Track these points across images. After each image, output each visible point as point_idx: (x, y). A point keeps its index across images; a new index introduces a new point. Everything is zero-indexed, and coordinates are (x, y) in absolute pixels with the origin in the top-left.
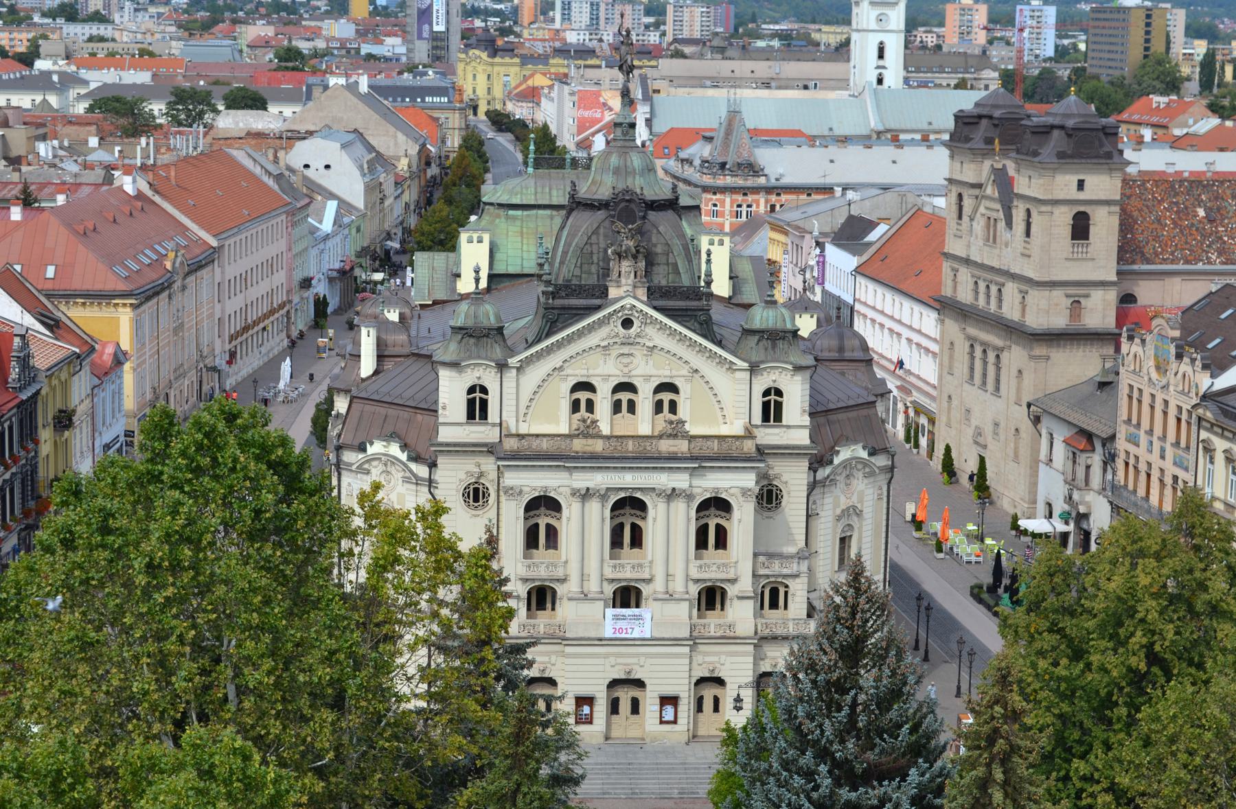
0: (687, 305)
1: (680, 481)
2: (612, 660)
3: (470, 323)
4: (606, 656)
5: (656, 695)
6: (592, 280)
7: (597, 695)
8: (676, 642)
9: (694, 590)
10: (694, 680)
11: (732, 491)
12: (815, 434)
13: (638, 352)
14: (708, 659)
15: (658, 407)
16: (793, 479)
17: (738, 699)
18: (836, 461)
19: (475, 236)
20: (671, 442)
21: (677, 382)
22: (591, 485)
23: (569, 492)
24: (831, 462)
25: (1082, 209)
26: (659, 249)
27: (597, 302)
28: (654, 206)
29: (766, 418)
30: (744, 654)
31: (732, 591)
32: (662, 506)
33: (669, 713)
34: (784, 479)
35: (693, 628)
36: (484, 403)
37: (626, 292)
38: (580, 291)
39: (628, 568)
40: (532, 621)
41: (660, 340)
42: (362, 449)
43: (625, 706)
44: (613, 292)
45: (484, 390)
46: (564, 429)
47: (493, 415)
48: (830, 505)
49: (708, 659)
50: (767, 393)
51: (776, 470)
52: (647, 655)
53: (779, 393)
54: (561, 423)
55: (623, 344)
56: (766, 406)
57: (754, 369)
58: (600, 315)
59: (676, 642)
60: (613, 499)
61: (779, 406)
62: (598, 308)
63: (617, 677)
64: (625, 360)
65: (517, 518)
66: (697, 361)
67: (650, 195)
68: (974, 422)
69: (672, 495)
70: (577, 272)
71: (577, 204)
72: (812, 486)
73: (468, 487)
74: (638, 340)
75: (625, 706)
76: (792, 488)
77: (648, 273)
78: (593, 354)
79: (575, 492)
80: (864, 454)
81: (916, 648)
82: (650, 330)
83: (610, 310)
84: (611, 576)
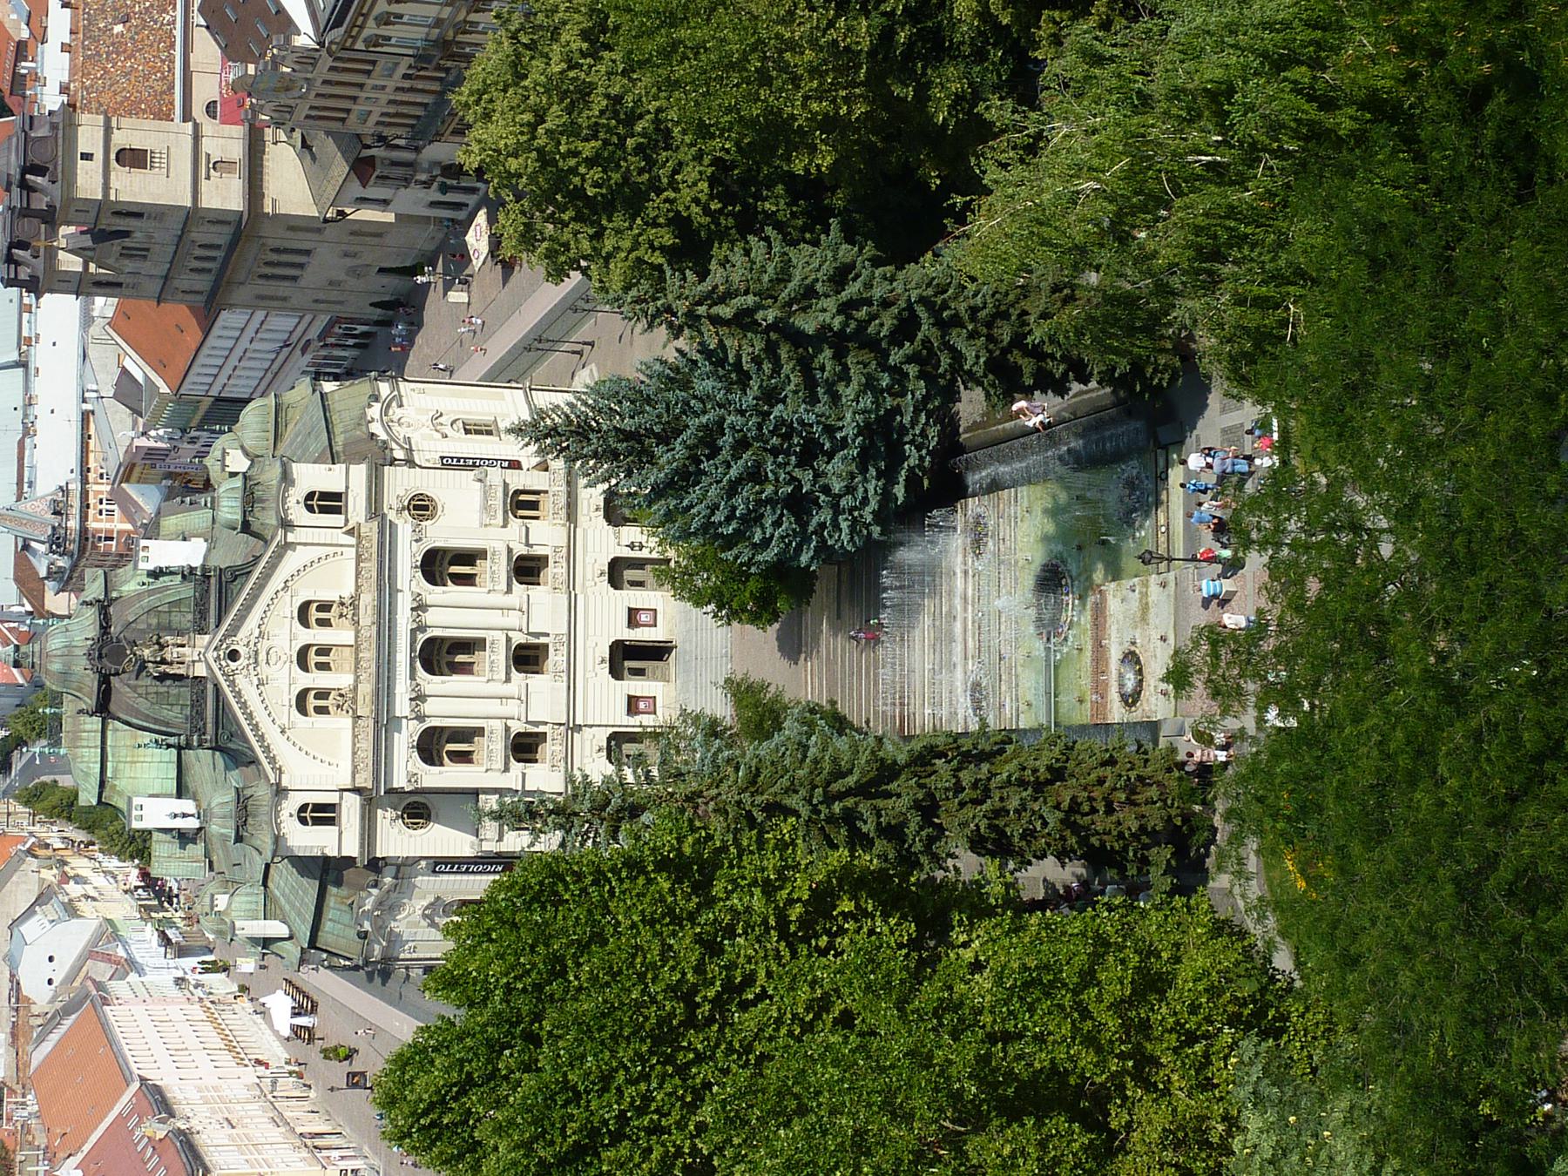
0: (216, 593)
1: (404, 604)
3: (232, 823)
4: (585, 680)
6: (186, 692)
12: (352, 458)
13: (263, 646)
15: (324, 623)
16: (400, 484)
17: (632, 546)
18: (383, 436)
19: (135, 813)
21: (298, 602)
24: (384, 442)
25: (113, 156)
26: (154, 621)
27: (210, 687)
28: (105, 628)
29: (337, 510)
31: (520, 550)
33: (644, 618)
36: (318, 807)
37: (196, 655)
38: (198, 703)
42: (363, 936)
44: (200, 670)
45: (303, 808)
46: (347, 722)
47: (332, 798)
48: (430, 448)
50: (310, 509)
53: (310, 496)
54: (339, 725)
56: (324, 510)
57: (287, 525)
58: (224, 685)
61: (325, 496)
62: (217, 687)
66: (276, 582)
67: (93, 632)
68: (342, 277)
70: (177, 709)
71: (103, 707)
72: (410, 463)
73: (406, 824)
77: (180, 633)
78: (265, 695)
80: (377, 406)
81: (580, 353)
82: (243, 633)
83: (219, 674)
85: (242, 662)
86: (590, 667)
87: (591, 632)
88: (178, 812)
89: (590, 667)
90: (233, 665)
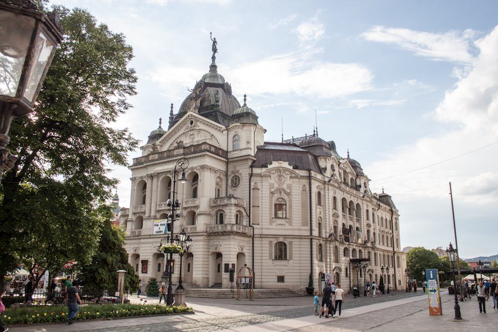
2: (154, 245)
13: (195, 132)
20: (177, 151)
22: (152, 172)
24: (266, 167)
34: (240, 172)
41: (201, 126)
51: (237, 168)
55: (191, 130)
64: (192, 137)
74: (195, 128)
80: (291, 168)
82: (199, 124)
84: (158, 209)
88: (162, 121)
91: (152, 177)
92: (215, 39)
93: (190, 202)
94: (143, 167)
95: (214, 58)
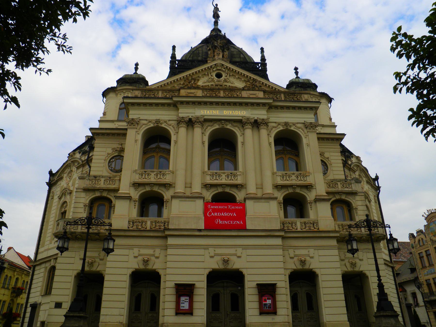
1: (260, 114)
2: (212, 251)
4: (206, 247)
5: (254, 284)
7: (197, 285)
8: (269, 234)
9: (280, 195)
10: (288, 272)
11: (299, 125)
14: (298, 252)
23: (175, 123)
26: (235, 53)
30: (330, 248)
31: (310, 196)
32: (249, 132)
35: (283, 223)
39: (224, 176)
40: (141, 219)
43: (225, 302)
49: (298, 252)
52: (245, 247)
59: (269, 234)
60: (209, 130)
63: (216, 267)
65: (136, 141)
69: (256, 124)
75: (225, 302)
76: (332, 161)
79: (180, 121)
82: (232, 79)
85: (216, 79)
86: (219, 251)
87: (250, 252)
89: (219, 251)
90: (214, 74)
91: (190, 123)
92: (217, 5)
93: (294, 177)
94: (169, 105)
95: (216, 23)
